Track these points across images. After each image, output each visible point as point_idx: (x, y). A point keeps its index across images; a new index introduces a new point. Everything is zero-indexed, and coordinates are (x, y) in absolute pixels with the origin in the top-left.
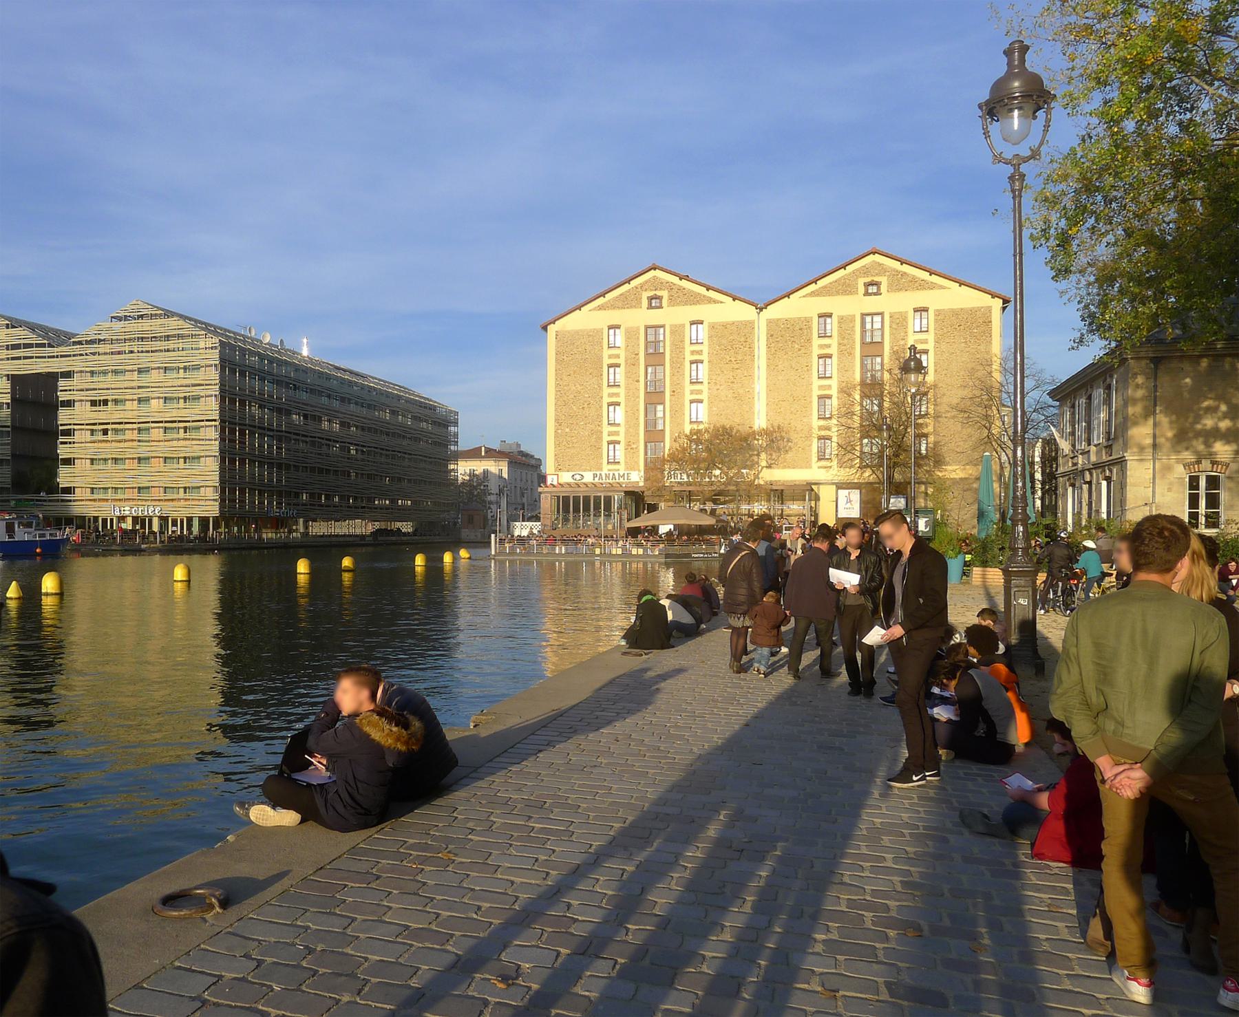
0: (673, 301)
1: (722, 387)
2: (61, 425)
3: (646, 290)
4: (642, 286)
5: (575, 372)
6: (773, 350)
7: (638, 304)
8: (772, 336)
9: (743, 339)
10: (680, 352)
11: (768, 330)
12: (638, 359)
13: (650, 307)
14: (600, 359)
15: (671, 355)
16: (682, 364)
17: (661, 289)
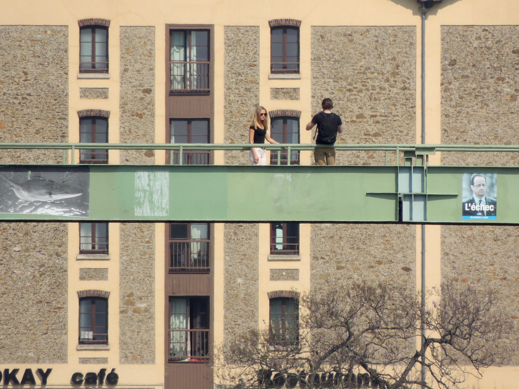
6: (456, 96)
8: (453, 63)
9: (389, 67)
11: (445, 51)
12: (151, 103)
15: (226, 96)
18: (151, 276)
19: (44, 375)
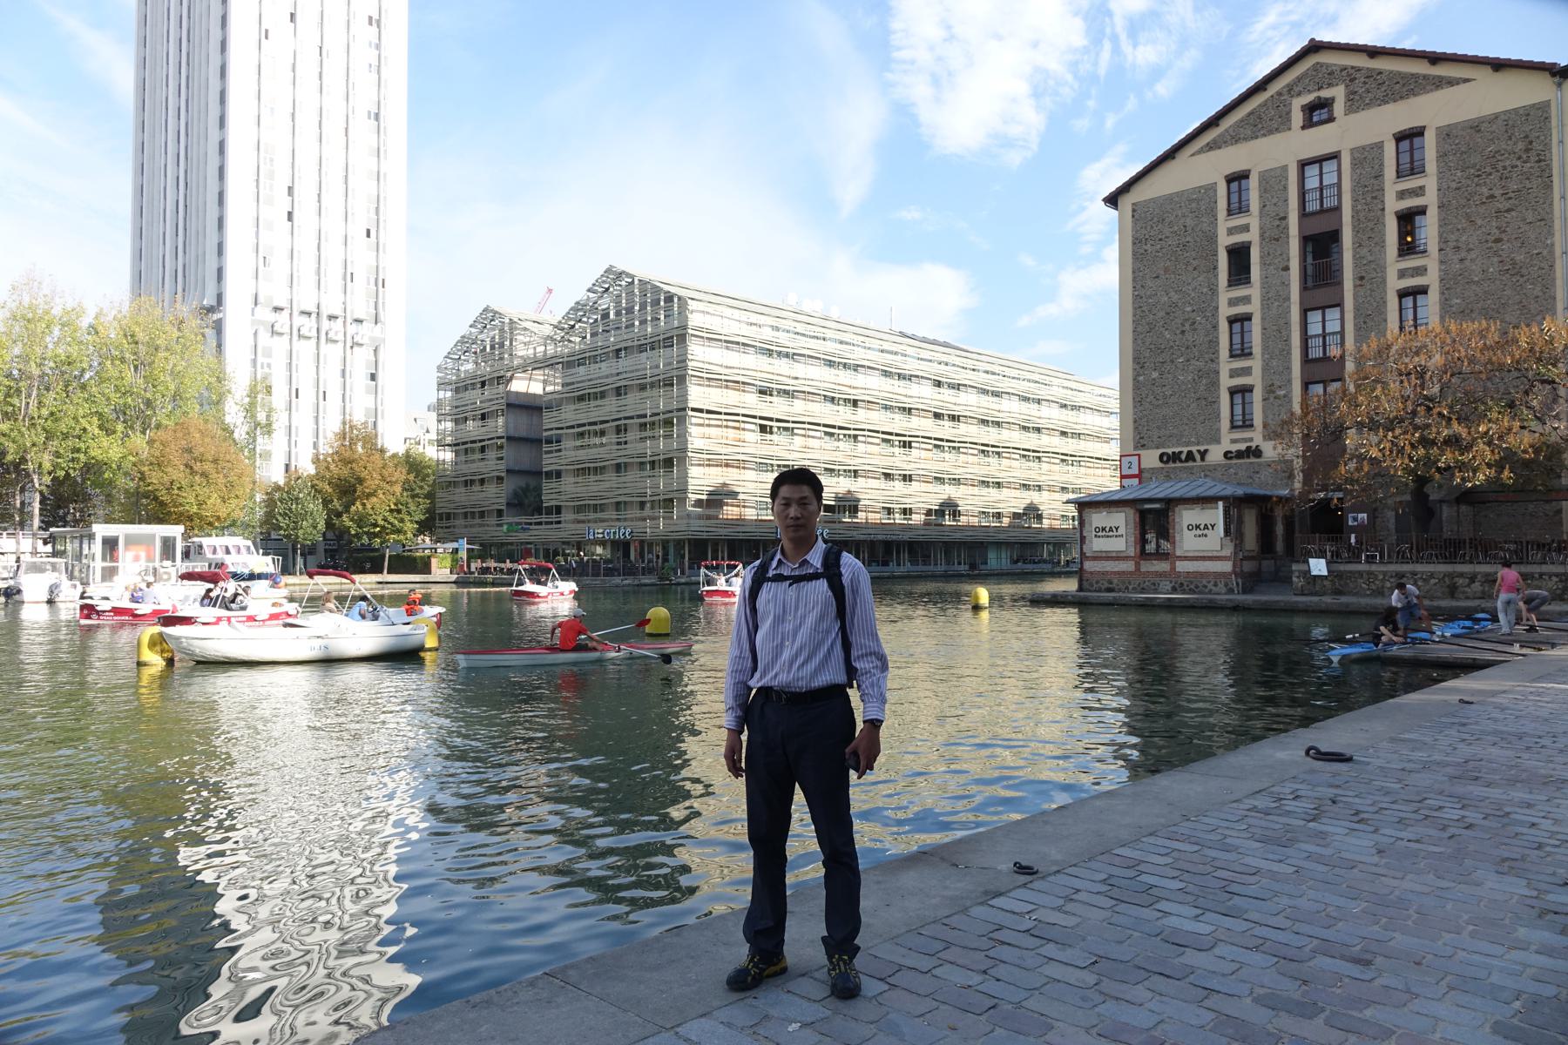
0: (1354, 105)
1: (1473, 255)
2: (546, 430)
3: (1299, 94)
4: (1290, 88)
5: (1166, 270)
7: (1284, 123)
9: (1521, 145)
10: (1375, 198)
12: (1287, 227)
13: (1308, 124)
14: (1212, 239)
15: (1353, 207)
16: (1380, 221)
17: (1330, 85)
18: (1289, 369)
19: (1203, 454)
